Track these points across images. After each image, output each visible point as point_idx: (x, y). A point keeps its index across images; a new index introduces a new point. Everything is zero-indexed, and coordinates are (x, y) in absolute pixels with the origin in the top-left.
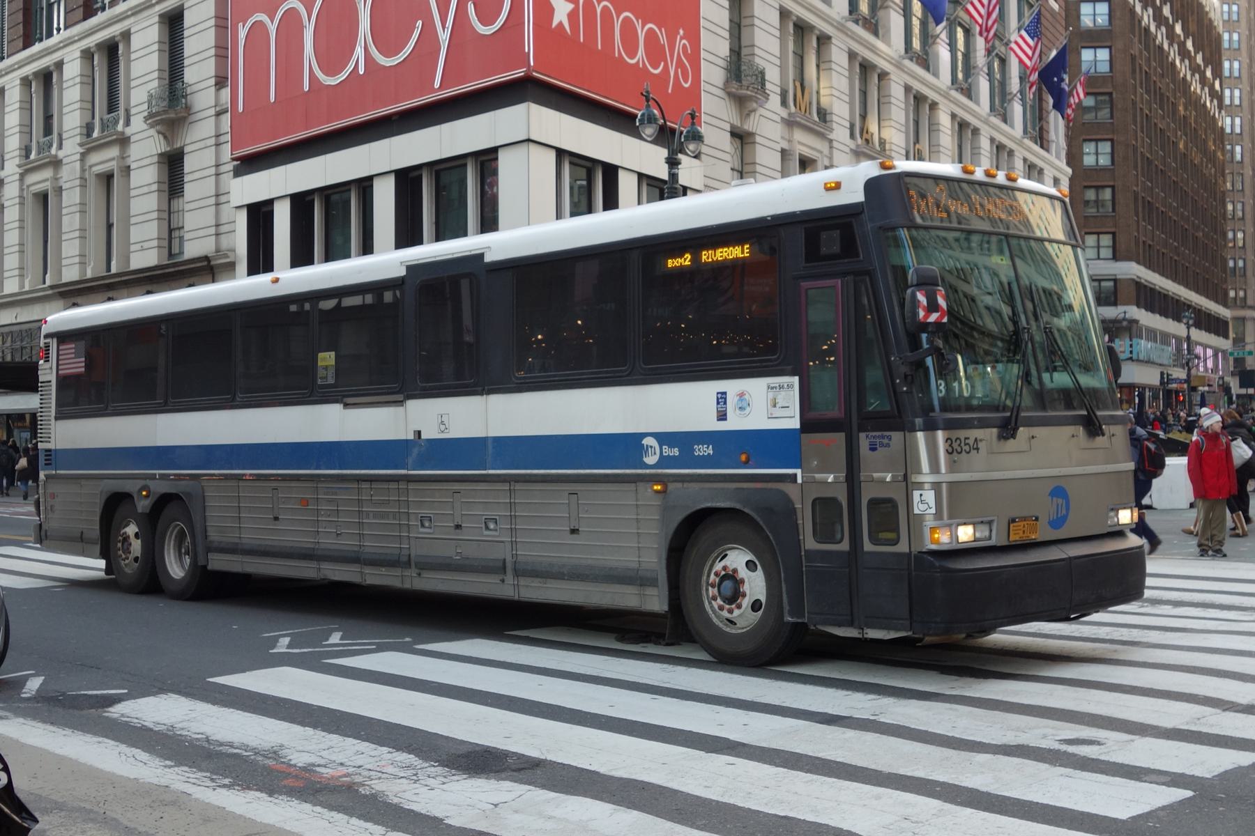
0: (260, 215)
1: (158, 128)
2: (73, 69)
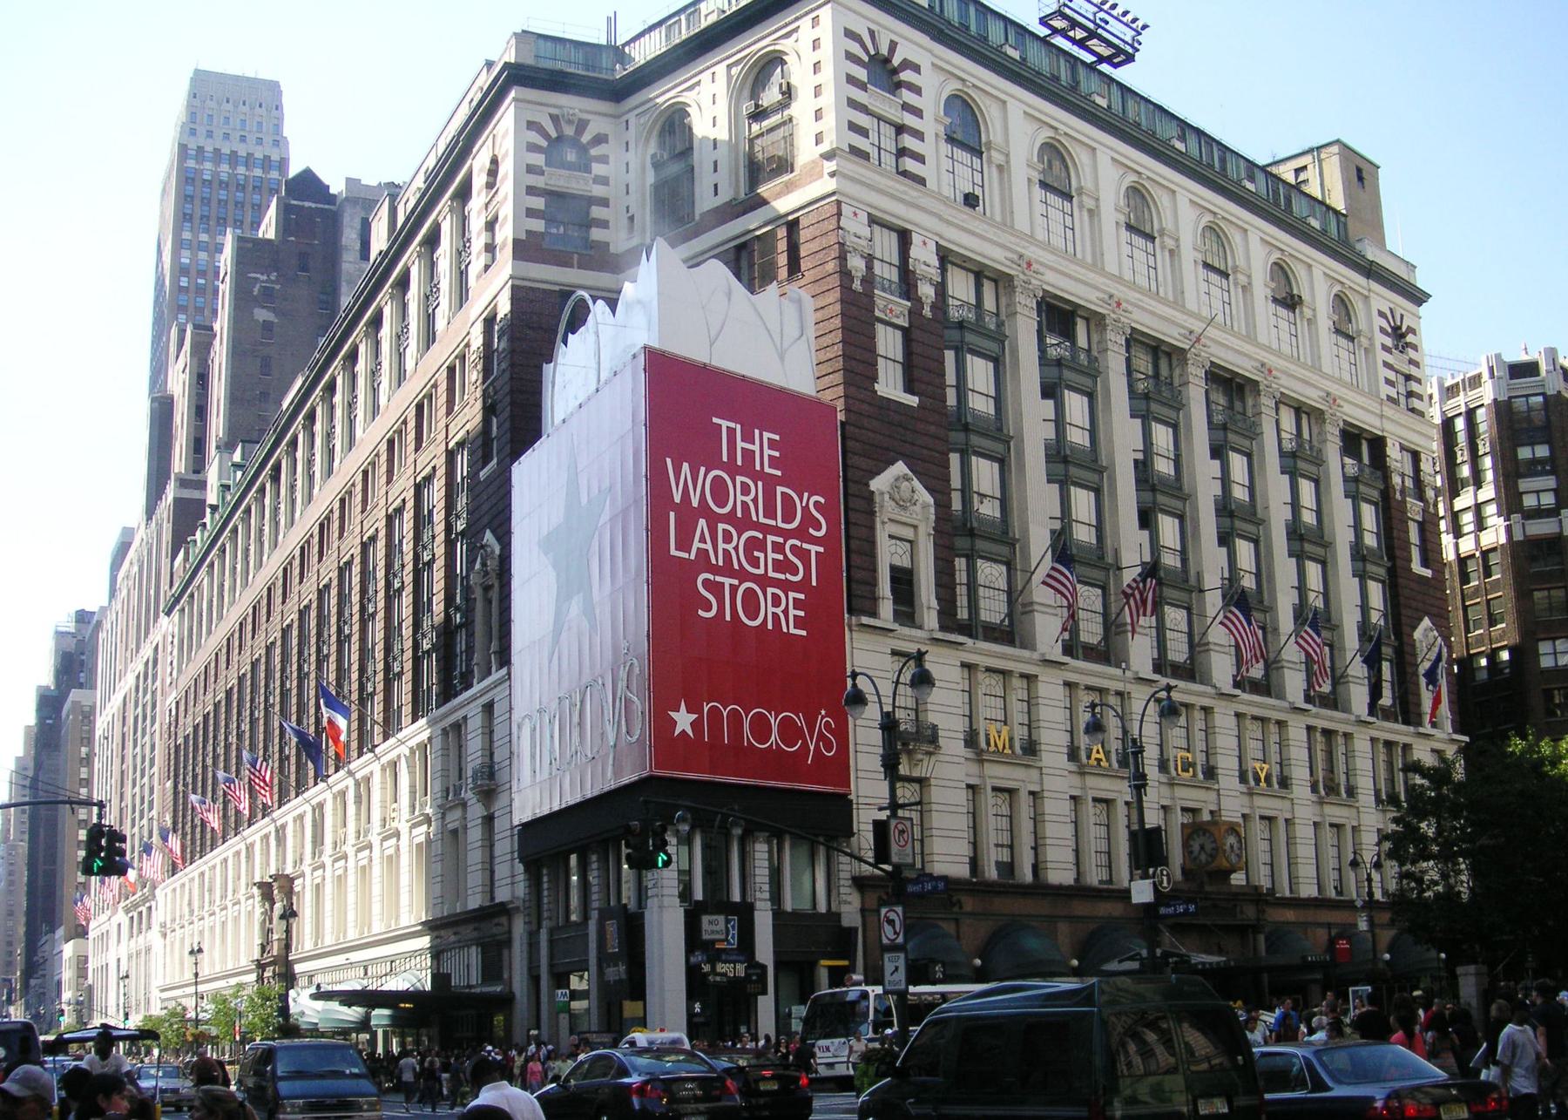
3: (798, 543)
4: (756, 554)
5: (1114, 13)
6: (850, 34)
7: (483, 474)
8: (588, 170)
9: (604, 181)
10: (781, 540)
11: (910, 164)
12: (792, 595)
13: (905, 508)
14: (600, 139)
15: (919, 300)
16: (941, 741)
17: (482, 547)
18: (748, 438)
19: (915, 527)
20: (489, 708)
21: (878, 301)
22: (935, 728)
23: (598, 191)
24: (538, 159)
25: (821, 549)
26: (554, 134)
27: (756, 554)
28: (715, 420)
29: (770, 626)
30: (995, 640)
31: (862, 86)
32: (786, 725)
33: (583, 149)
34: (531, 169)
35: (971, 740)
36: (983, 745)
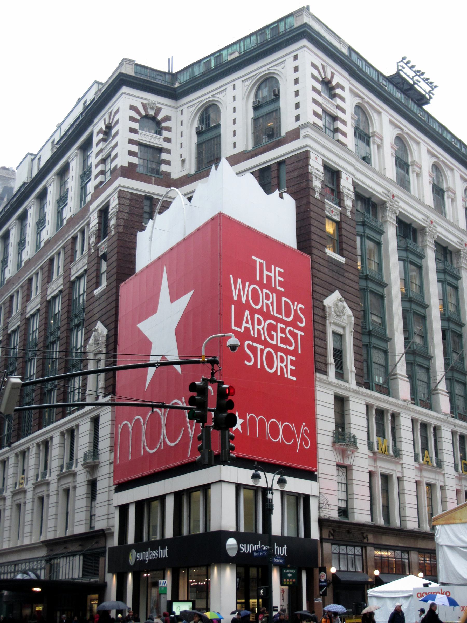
0: (124, 509)
1: (87, 469)
2: (57, 440)
3: (292, 329)
4: (273, 333)
5: (422, 77)
6: (313, 65)
7: (97, 292)
8: (160, 134)
9: (168, 140)
10: (284, 326)
11: (340, 137)
12: (290, 357)
14: (167, 118)
15: (344, 208)
16: (358, 445)
17: (96, 330)
18: (269, 269)
19: (344, 328)
20: (96, 421)
21: (327, 206)
22: (354, 437)
23: (165, 145)
24: (135, 126)
25: (303, 334)
26: (144, 114)
27: (273, 333)
28: (254, 257)
29: (279, 374)
30: (380, 392)
31: (319, 93)
32: (286, 428)
33: (158, 123)
34: (132, 130)
35: (370, 446)
36: (376, 449)
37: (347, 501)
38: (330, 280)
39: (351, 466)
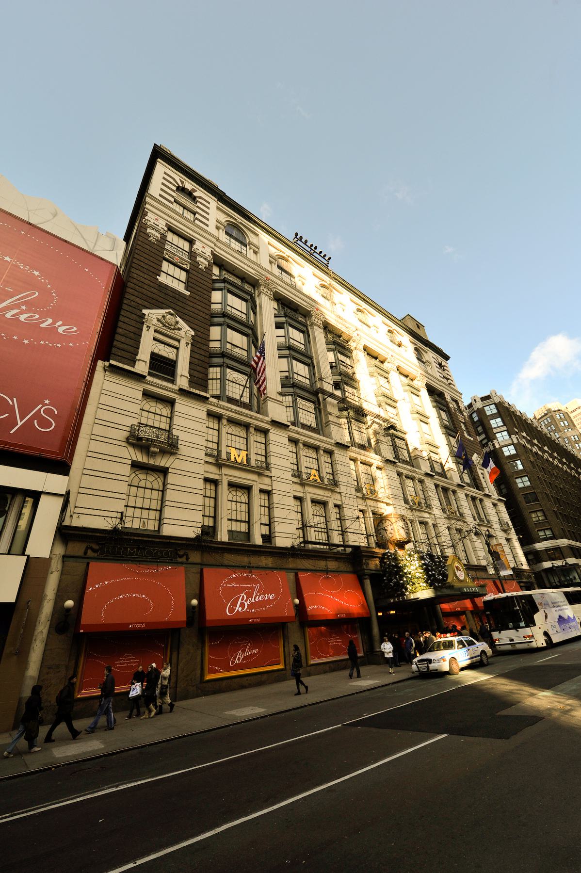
13: (169, 328)
16: (179, 446)
19: (179, 341)
37: (161, 511)
38: (161, 299)
39: (167, 469)
